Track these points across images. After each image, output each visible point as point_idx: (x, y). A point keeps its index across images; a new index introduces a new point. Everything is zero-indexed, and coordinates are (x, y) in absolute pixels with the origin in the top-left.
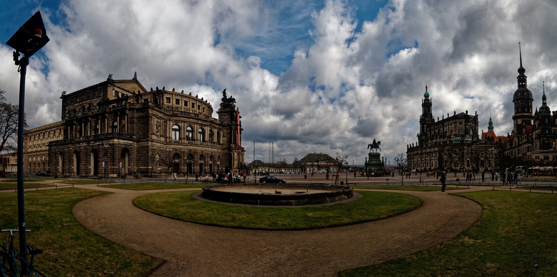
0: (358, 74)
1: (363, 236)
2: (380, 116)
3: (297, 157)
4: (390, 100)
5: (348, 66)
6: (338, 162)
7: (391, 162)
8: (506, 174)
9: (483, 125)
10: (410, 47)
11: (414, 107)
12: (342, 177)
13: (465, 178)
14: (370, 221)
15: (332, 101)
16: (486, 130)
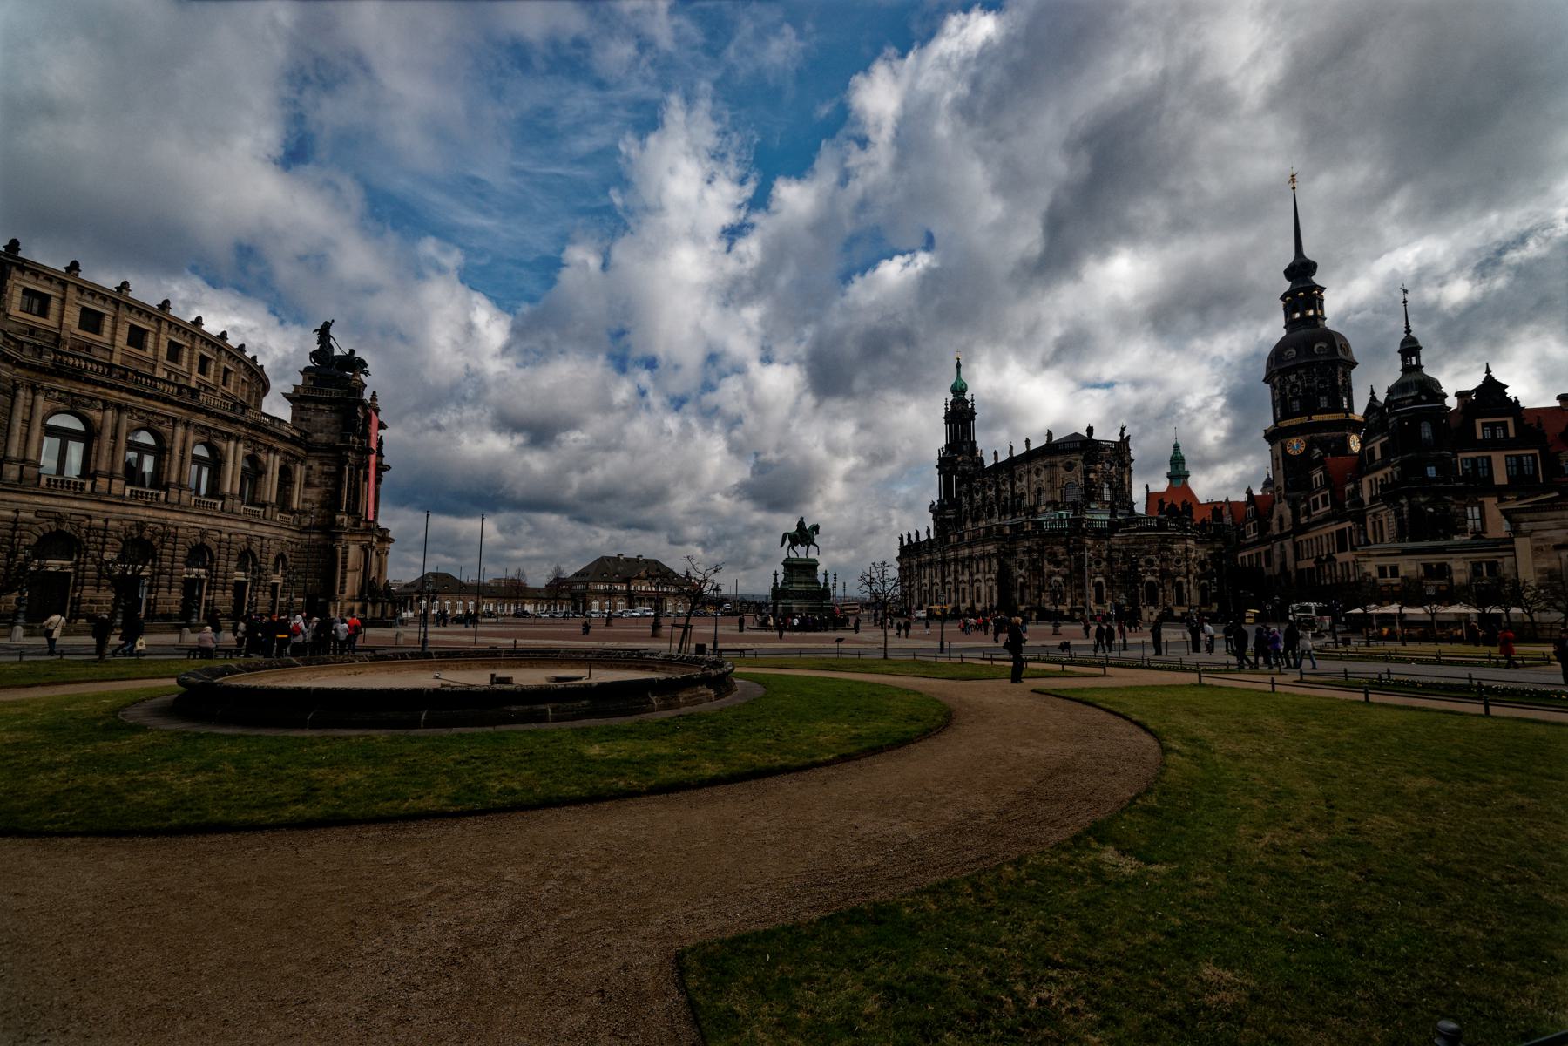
0: (756, 329)
1: (763, 823)
2: (820, 452)
3: (563, 566)
4: (849, 403)
5: (726, 305)
6: (690, 583)
7: (849, 588)
8: (1250, 628)
9: (1151, 468)
10: (911, 251)
11: (920, 424)
12: (702, 629)
13: (1092, 641)
14: (785, 770)
15: (677, 403)
16: (1161, 485)
